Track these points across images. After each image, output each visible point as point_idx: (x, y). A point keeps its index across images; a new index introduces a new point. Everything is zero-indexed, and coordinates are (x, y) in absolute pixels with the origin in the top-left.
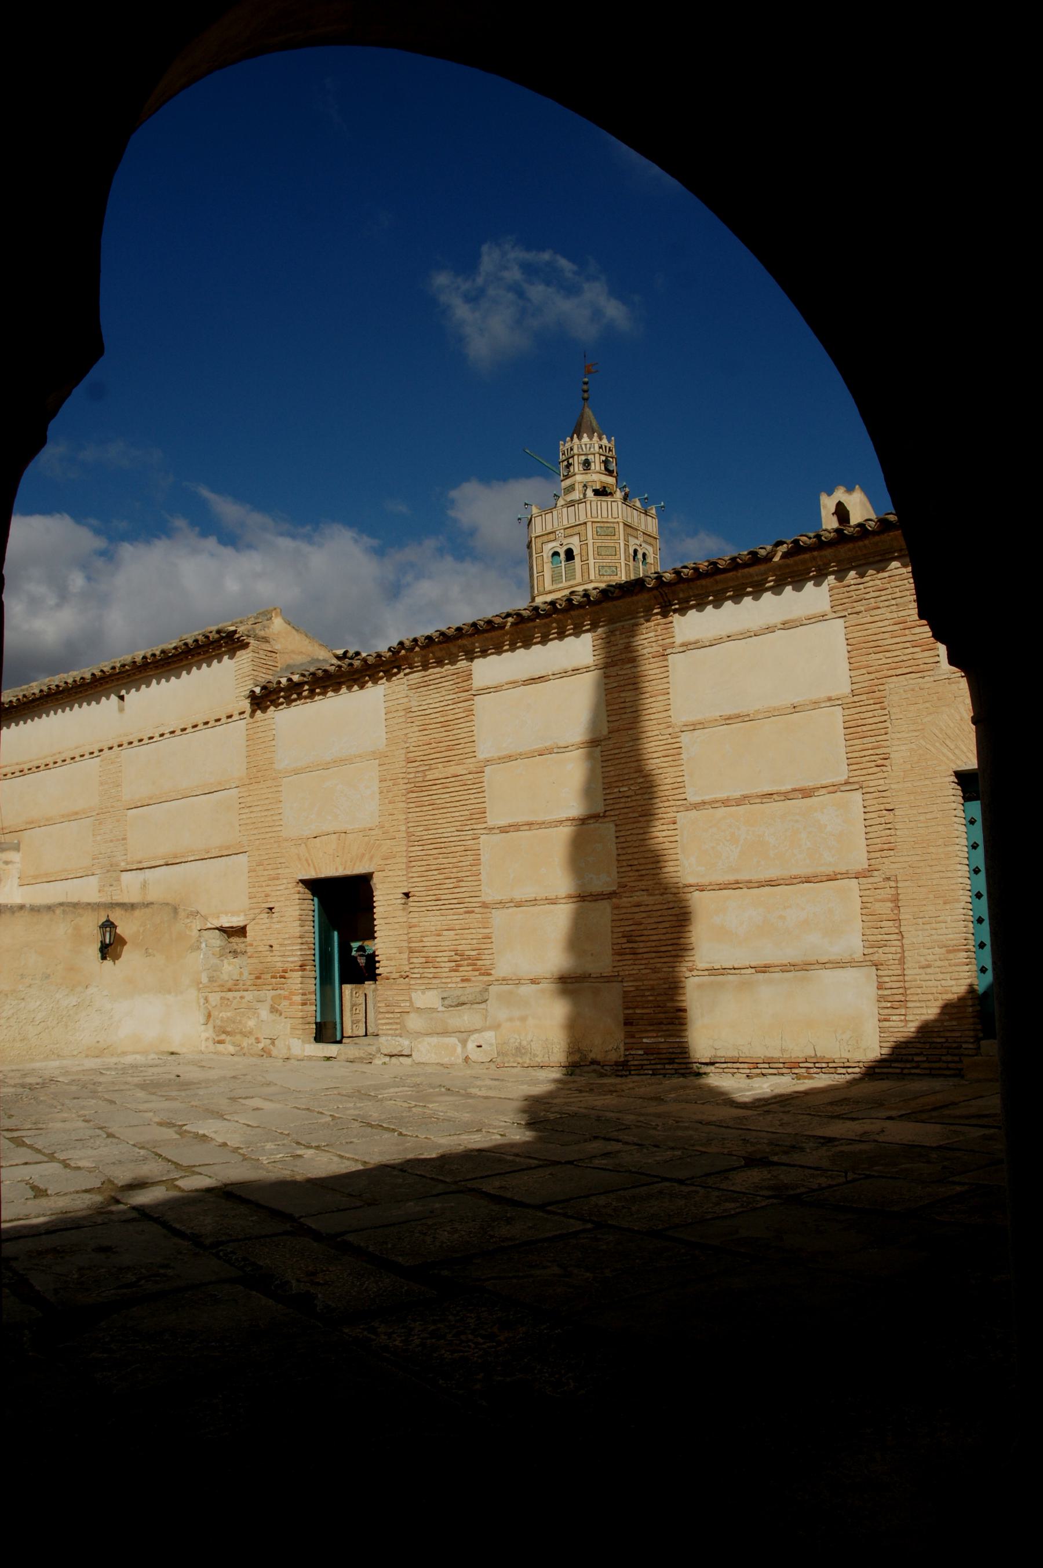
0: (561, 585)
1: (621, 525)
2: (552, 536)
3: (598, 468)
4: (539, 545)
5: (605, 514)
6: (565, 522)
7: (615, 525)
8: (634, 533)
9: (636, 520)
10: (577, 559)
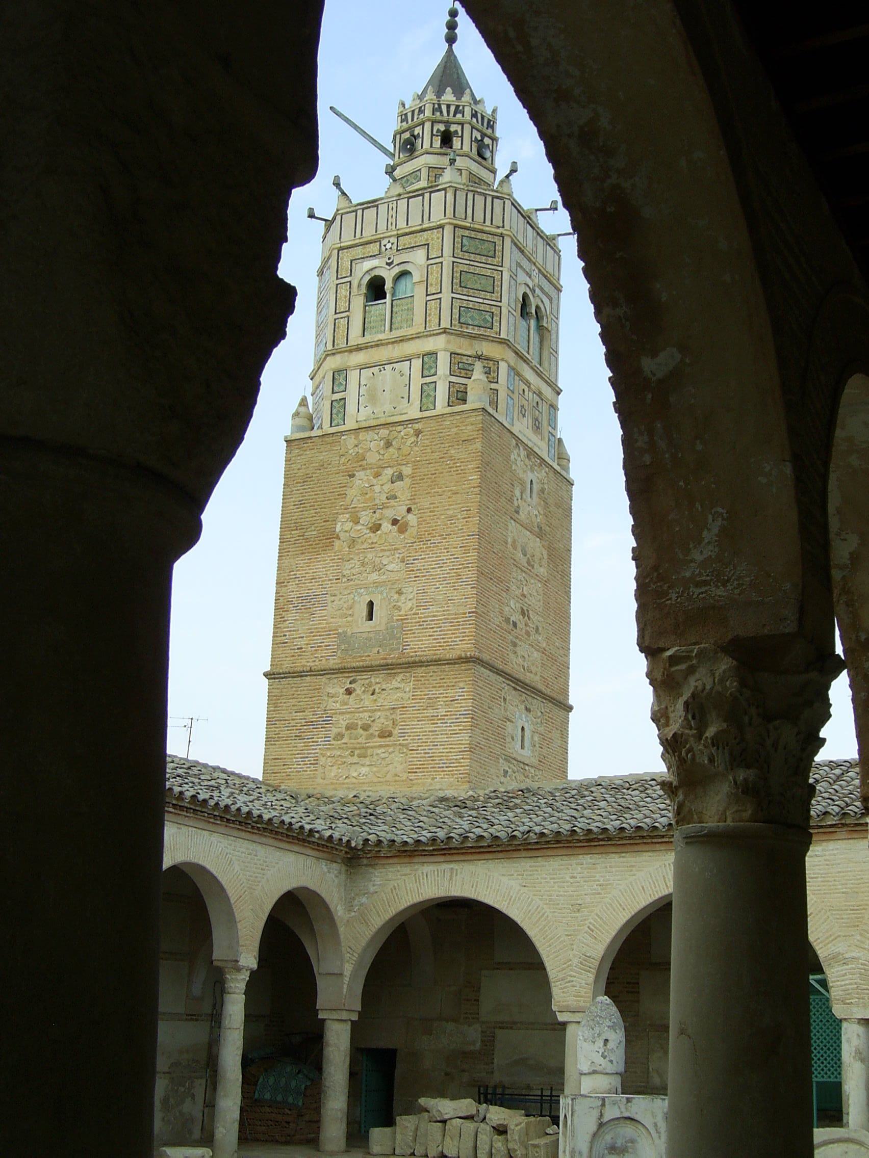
2: (374, 249)
3: (466, 148)
5: (479, 216)
7: (496, 239)
8: (525, 264)
9: (530, 243)
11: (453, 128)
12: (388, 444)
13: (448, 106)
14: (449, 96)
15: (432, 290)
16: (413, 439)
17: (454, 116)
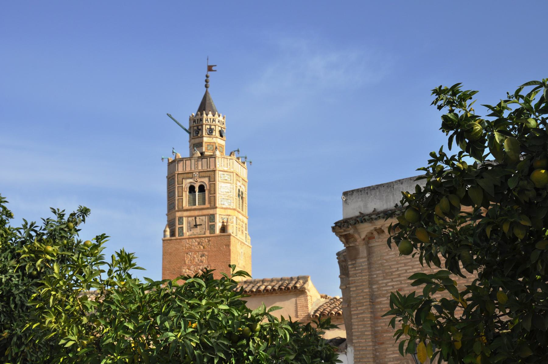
0: (194, 207)
1: (235, 174)
2: (190, 175)
4: (180, 179)
6: (200, 168)
10: (207, 192)
11: (212, 127)
12: (199, 244)
14: (210, 115)
15: (212, 192)
16: (208, 243)
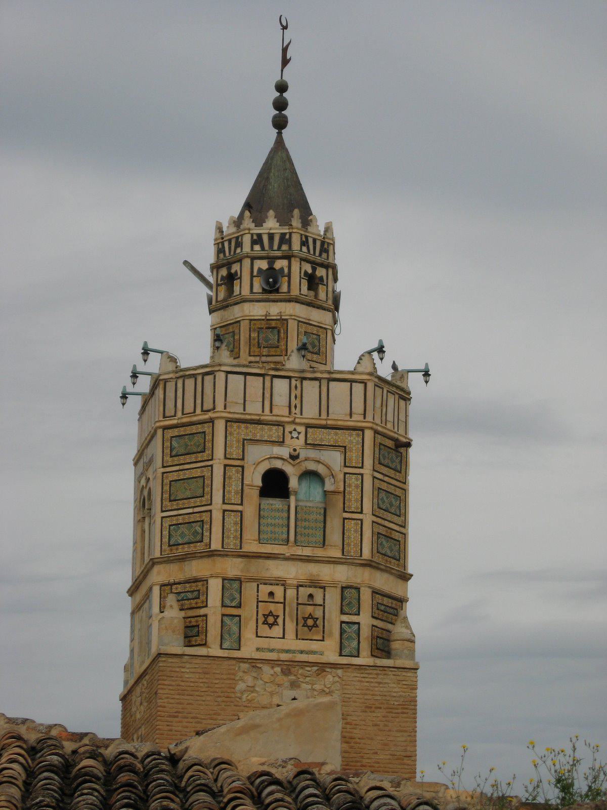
2: (274, 433)
13: (314, 241)
17: (320, 255)
